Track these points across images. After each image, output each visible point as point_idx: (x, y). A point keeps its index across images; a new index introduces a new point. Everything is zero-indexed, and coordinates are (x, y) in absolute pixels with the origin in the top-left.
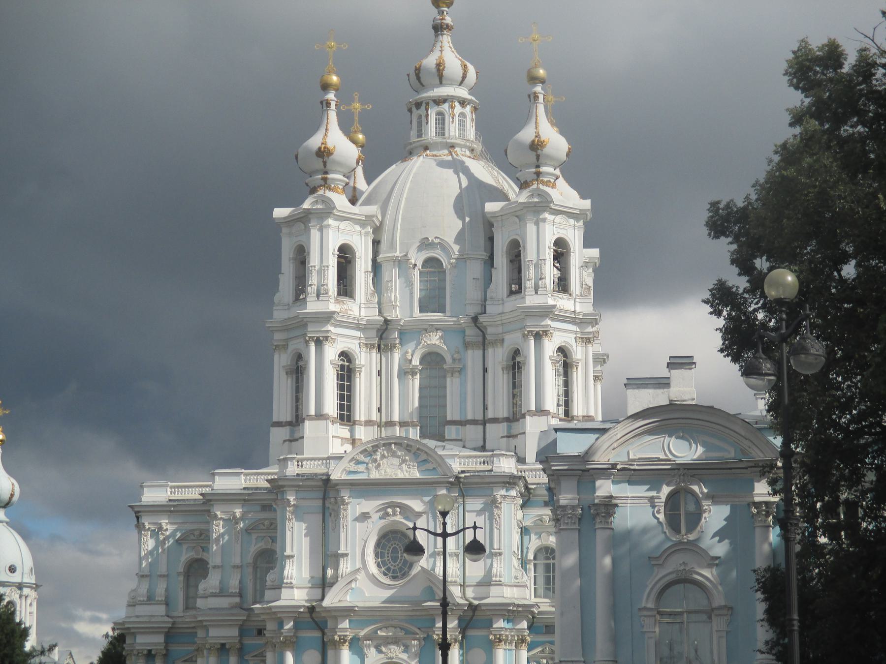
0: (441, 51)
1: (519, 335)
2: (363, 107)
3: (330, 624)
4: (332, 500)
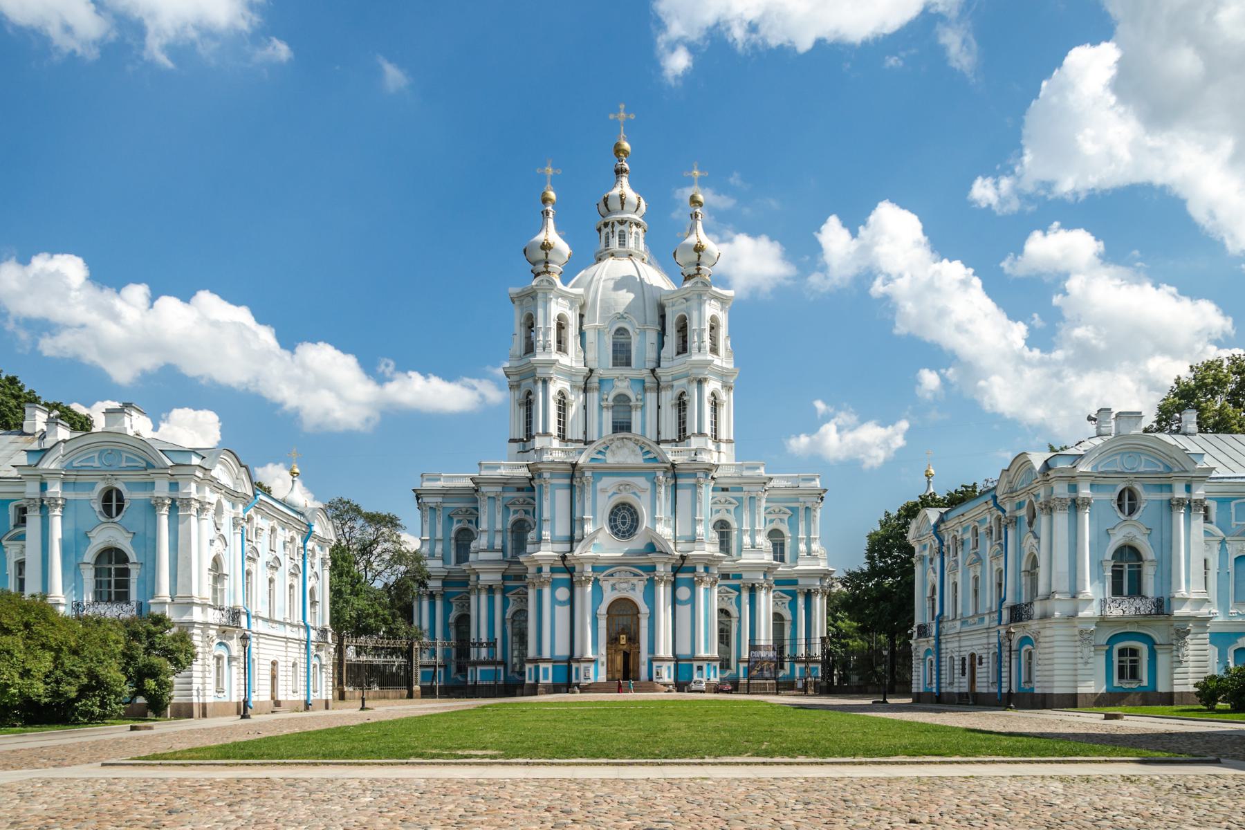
1: (684, 381)
3: (577, 569)
4: (578, 479)
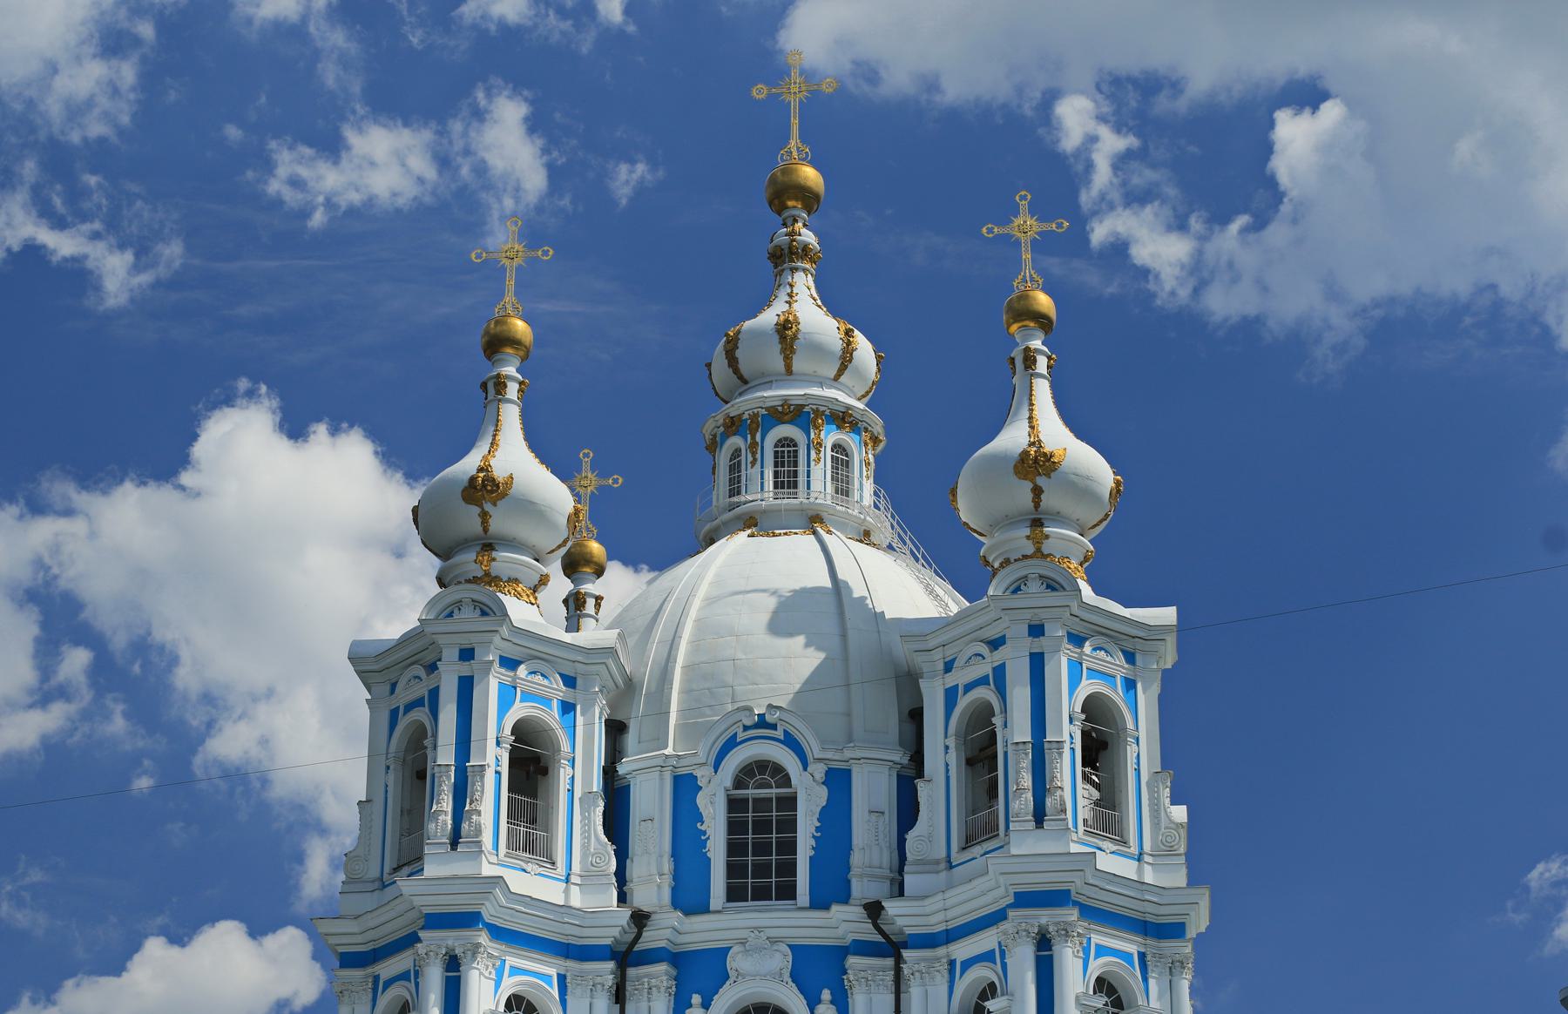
0: (787, 302)
2: (604, 483)
